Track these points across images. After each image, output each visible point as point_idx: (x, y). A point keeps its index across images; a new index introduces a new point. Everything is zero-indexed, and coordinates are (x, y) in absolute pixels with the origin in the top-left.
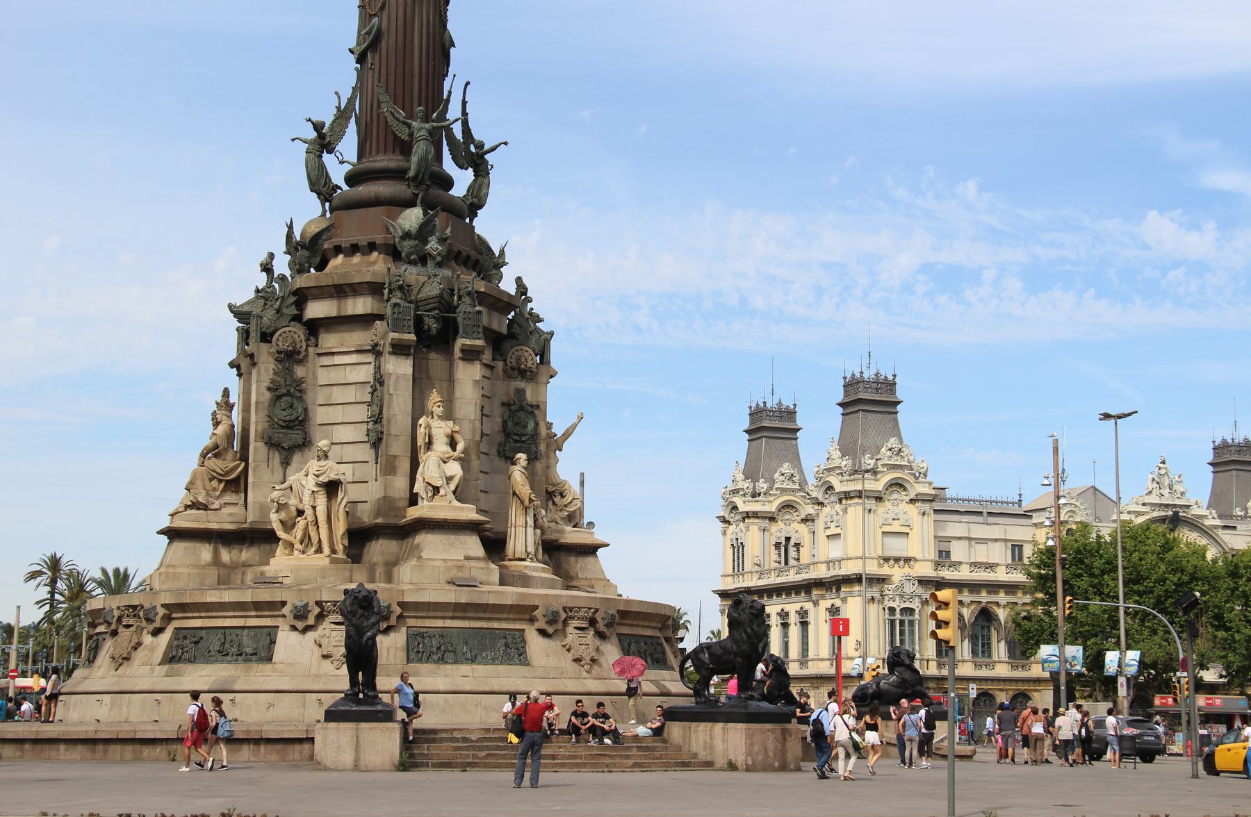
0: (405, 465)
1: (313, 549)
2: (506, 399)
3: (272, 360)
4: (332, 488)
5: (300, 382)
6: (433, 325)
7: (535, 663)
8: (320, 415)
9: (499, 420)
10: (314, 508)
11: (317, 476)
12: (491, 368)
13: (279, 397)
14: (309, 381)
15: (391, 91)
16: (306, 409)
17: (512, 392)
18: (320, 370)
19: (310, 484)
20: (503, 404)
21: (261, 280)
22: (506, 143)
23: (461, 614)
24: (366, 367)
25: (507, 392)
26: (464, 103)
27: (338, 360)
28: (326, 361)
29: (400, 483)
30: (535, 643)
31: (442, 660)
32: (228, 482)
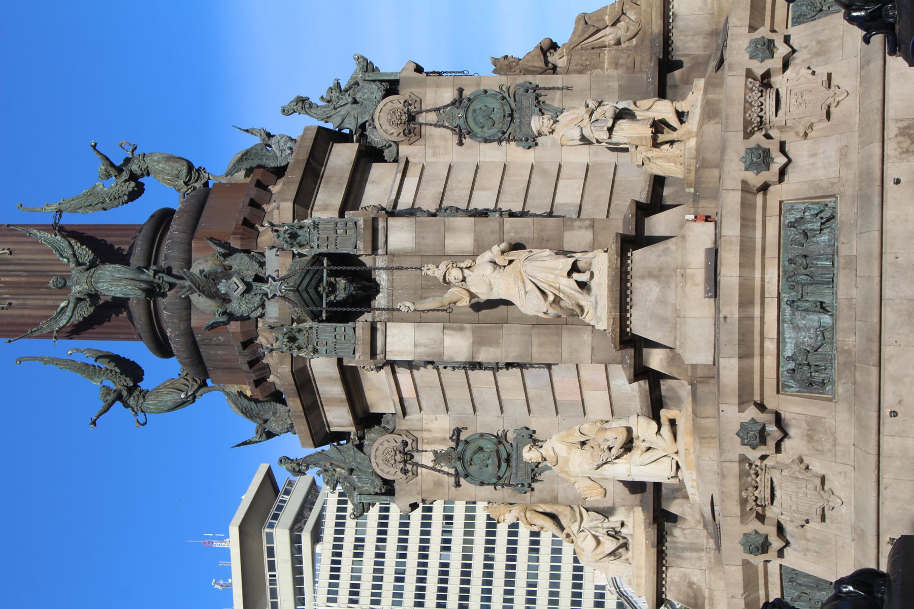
16: (482, 435)
20: (461, 143)
22: (94, 147)
27: (408, 391)
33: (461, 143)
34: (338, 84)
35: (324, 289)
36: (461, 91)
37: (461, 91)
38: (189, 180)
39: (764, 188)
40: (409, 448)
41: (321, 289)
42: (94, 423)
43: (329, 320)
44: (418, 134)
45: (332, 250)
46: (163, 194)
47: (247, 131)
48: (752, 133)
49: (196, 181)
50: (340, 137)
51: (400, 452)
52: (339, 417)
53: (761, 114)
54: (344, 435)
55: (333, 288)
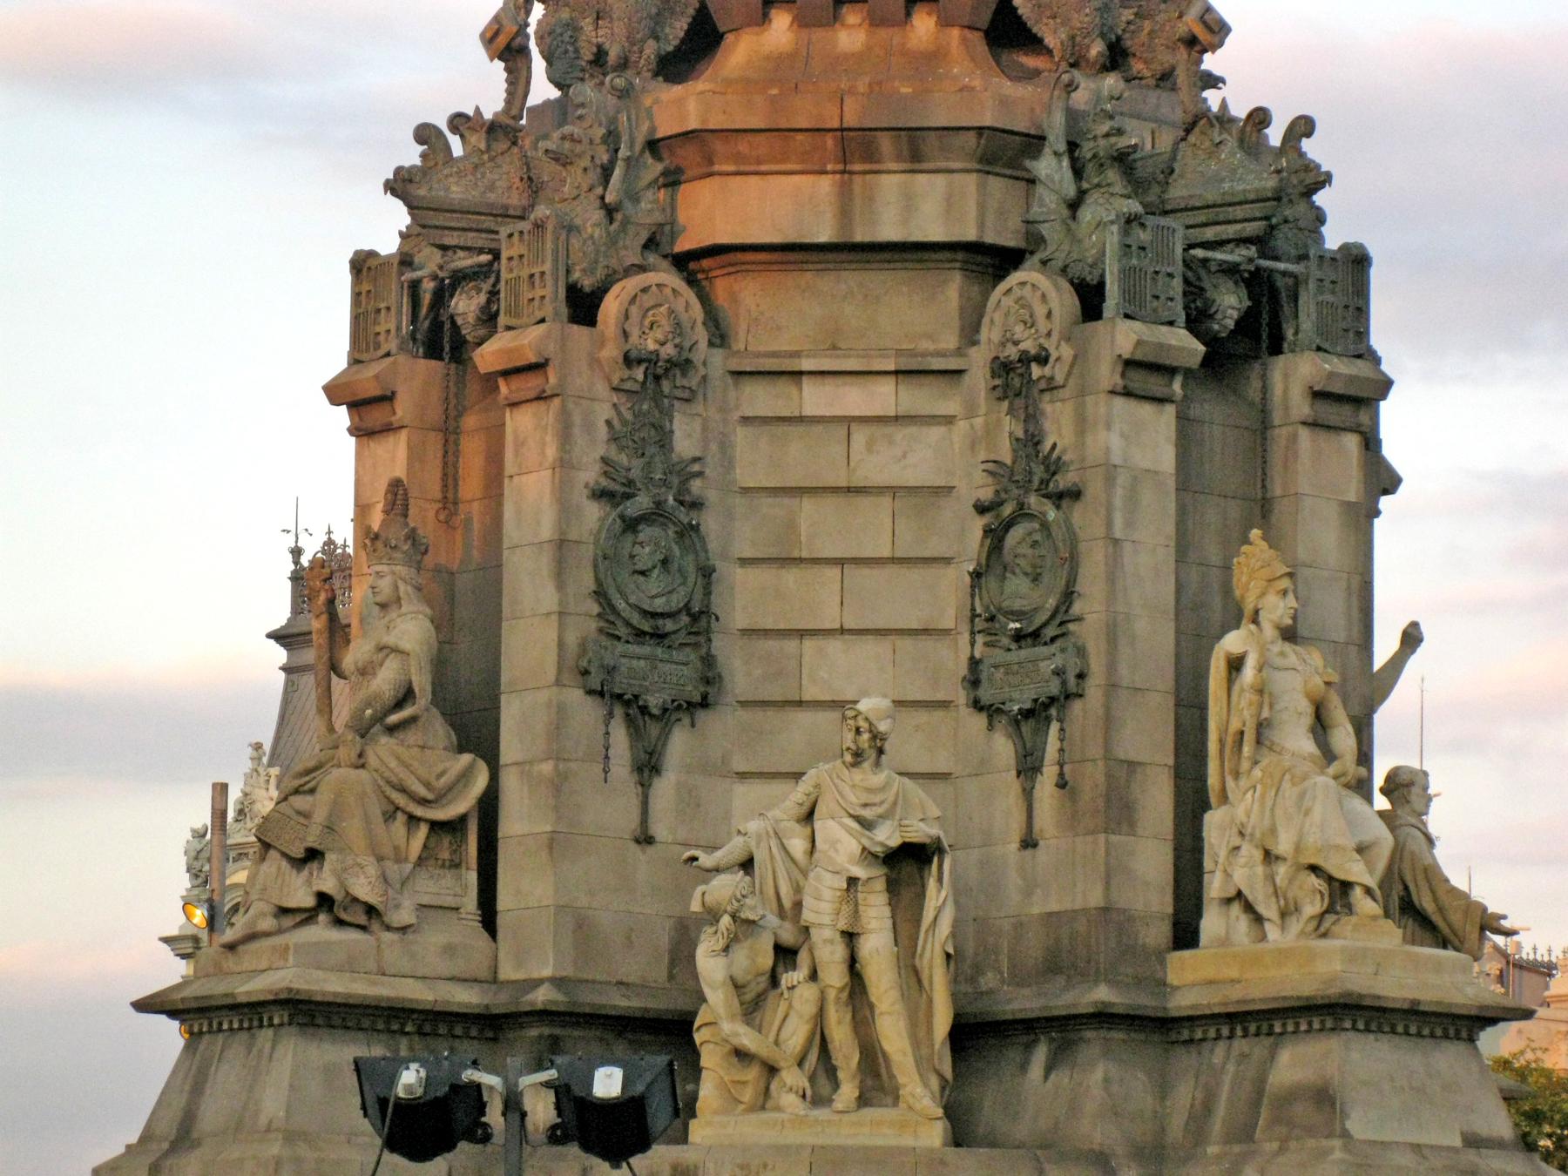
0: (1157, 800)
1: (848, 1091)
4: (908, 862)
5: (684, 473)
8: (745, 598)
10: (850, 937)
11: (867, 824)
13: (631, 525)
16: (707, 573)
18: (741, 436)
19: (842, 845)
21: (486, 89)
24: (936, 433)
27: (815, 399)
28: (761, 399)
29: (1152, 860)
32: (436, 826)
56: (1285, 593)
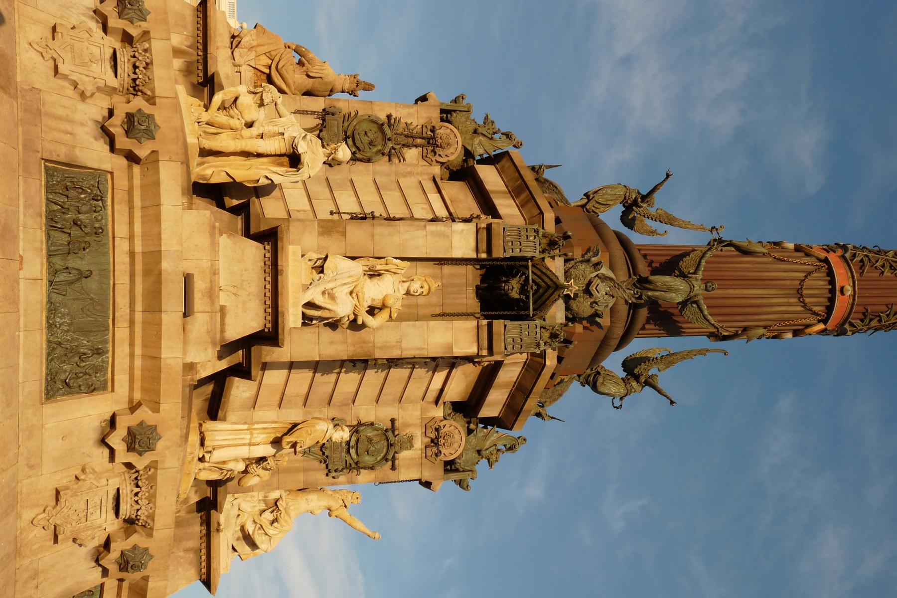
2: (397, 424)
3: (422, 121)
6: (513, 288)
7: (49, 409)
9: (371, 419)
12: (437, 402)
14: (402, 167)
15: (713, 259)
17: (408, 431)
20: (393, 421)
22: (672, 402)
23: (139, 267)
25: (407, 425)
26: (703, 352)
27: (434, 198)
30: (90, 411)
31: (52, 224)
33: (393, 421)
34: (490, 465)
35: (532, 288)
36: (393, 468)
37: (393, 468)
38: (595, 376)
39: (134, 407)
40: (430, 148)
41: (535, 287)
42: (668, 176)
43: (525, 259)
44: (428, 427)
45: (524, 323)
46: (613, 363)
47: (552, 418)
48: (148, 468)
49: (589, 376)
50: (488, 422)
51: (437, 146)
52: (489, 176)
53: (138, 490)
54: (482, 161)
55: (523, 290)
56: (422, 287)
